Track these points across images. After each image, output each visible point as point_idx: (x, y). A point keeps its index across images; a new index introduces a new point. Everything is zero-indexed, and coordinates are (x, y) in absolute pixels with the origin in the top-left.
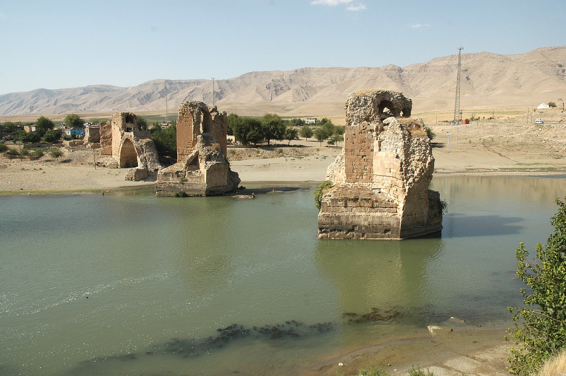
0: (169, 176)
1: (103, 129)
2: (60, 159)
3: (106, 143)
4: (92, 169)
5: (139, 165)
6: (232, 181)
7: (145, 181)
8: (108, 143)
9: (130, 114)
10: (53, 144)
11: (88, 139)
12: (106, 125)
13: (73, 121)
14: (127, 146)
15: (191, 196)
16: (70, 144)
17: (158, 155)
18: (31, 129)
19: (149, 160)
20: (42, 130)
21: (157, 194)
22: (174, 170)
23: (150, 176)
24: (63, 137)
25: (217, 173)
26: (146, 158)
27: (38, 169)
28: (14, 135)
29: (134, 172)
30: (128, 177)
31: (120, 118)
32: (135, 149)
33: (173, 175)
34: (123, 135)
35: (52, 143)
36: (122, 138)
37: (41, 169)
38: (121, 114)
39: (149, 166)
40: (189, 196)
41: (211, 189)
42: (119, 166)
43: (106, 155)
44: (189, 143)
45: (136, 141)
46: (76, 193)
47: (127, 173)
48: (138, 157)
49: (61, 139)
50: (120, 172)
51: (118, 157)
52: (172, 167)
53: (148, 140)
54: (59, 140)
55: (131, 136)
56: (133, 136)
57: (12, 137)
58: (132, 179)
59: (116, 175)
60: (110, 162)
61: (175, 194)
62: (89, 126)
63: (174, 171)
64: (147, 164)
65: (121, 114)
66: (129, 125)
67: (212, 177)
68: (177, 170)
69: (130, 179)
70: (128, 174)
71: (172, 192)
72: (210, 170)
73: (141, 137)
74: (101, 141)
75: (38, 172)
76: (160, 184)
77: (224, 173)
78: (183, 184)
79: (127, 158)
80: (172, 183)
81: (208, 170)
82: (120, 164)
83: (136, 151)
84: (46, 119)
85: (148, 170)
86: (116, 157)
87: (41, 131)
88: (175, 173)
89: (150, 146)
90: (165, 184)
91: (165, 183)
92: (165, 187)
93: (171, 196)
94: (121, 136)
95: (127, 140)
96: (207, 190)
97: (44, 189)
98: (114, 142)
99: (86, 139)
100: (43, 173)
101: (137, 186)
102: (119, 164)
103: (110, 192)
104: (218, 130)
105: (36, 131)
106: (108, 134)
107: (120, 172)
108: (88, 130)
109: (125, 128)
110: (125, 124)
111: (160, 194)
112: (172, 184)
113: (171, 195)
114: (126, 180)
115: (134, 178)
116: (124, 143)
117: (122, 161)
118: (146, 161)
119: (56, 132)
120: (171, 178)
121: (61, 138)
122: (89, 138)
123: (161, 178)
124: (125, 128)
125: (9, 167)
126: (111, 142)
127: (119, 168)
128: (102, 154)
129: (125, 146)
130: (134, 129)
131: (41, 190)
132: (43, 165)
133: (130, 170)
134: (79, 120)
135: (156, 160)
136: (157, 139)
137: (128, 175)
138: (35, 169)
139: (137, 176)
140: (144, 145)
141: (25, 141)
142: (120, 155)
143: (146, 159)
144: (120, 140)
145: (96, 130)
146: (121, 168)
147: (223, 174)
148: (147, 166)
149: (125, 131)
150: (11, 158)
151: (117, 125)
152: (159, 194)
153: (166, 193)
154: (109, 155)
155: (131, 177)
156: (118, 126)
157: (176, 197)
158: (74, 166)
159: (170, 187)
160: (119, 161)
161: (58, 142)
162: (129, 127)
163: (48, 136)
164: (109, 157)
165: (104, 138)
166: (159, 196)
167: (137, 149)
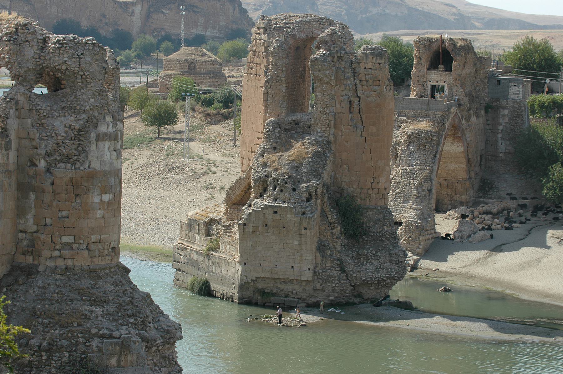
6: (343, 270)
15: (218, 297)
25: (274, 237)
40: (215, 297)
41: (260, 285)
44: (258, 138)
67: (260, 248)
68: (211, 215)
72: (251, 225)
77: (300, 241)
78: (208, 256)
81: (245, 225)
96: (243, 287)
104: (338, 106)
130: (450, 88)
140: (405, 141)
147: (296, 243)
162: (435, 83)
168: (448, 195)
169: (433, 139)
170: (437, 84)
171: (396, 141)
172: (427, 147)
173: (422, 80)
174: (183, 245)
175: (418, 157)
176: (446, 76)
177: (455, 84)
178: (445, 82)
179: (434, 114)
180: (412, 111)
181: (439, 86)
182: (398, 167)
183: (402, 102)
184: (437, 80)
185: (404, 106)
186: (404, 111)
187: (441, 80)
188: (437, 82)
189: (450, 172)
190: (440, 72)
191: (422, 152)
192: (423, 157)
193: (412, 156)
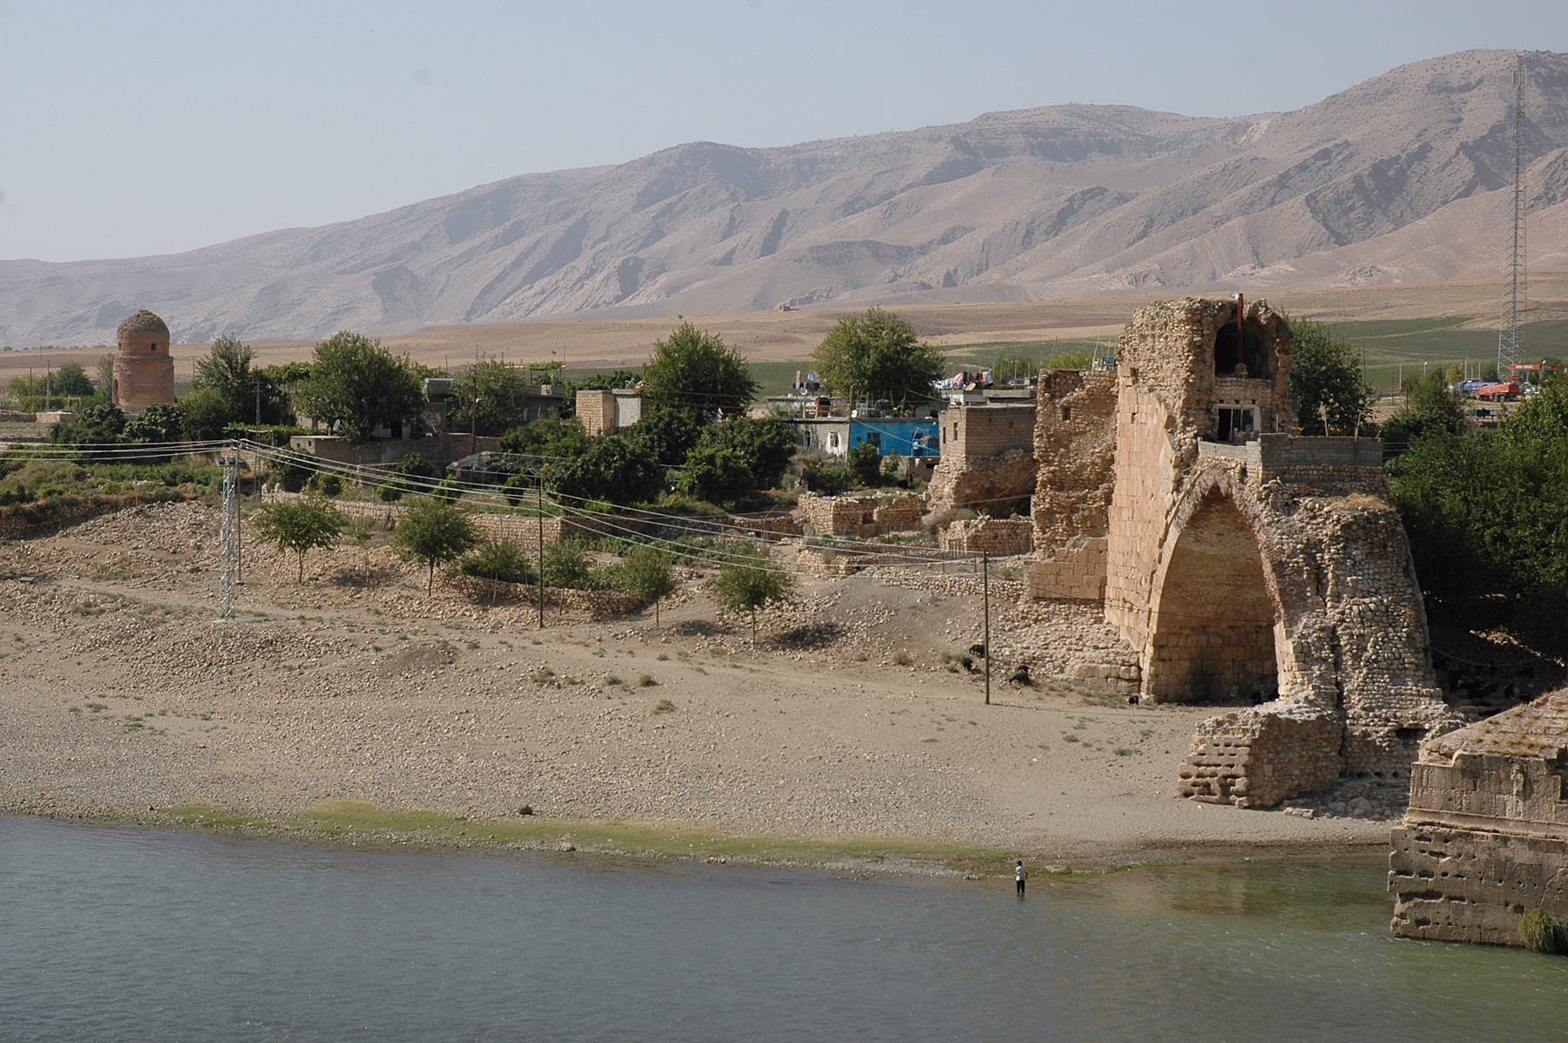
0: (1502, 783)
1: (1060, 415)
2: (768, 618)
3: (1069, 518)
4: (962, 695)
5: (1282, 690)
7: (1315, 815)
8: (1085, 519)
9: (1247, 309)
10: (738, 519)
11: (957, 490)
12: (1079, 393)
13: (869, 363)
14: (1210, 545)
16: (841, 516)
17: (1424, 618)
18: (616, 409)
19: (1356, 658)
20: (680, 420)
21: (1403, 916)
22: (1544, 741)
23: (1361, 775)
24: (801, 467)
26: (1338, 639)
27: (633, 679)
28: (516, 446)
29: (1246, 739)
30: (1199, 776)
31: (1179, 338)
32: (1267, 568)
33: (1528, 784)
34: (1185, 462)
35: (731, 512)
36: (1177, 489)
37: (649, 683)
38: (1182, 315)
39: (1355, 698)
42: (1144, 685)
43: (1060, 601)
45: (1274, 507)
46: (849, 864)
47: (1194, 744)
48: (1279, 630)
49: (783, 482)
50: (1146, 734)
51: (1143, 625)
52: (1526, 720)
53: (1363, 502)
54: (773, 492)
55: (1244, 472)
56: (1256, 469)
57: (505, 459)
58: (1225, 790)
59: (1122, 753)
60: (1088, 653)
61: (1537, 930)
62: (966, 393)
63: (1543, 747)
64: (1339, 685)
65: (1190, 311)
66: (1235, 393)
69: (1215, 786)
70: (1201, 748)
71: (1519, 909)
73: (1311, 484)
74: (1038, 503)
75: (629, 699)
76: (1430, 845)
79: (1203, 629)
80: (1522, 840)
82: (1155, 676)
83: (1272, 586)
84: (707, 348)
85: (1345, 729)
86: (1129, 619)
87: (669, 425)
88: (1549, 762)
89: (1377, 551)
90: (1469, 848)
91: (1467, 836)
92: (1467, 868)
93: (1503, 945)
94: (1172, 473)
95: (1214, 503)
97: (656, 823)
98: (1126, 514)
99: (943, 487)
100: (661, 709)
101: (1259, 846)
102: (1145, 675)
103: (1069, 872)
105: (645, 427)
106: (1087, 454)
107: (1146, 734)
108: (962, 425)
109: (1208, 411)
110: (1205, 384)
111: (1425, 922)
112: (1519, 846)
113: (1507, 938)
114: (1187, 795)
115: (1240, 784)
116: (1194, 521)
117: (1165, 654)
118: (1337, 665)
119: (760, 434)
120: (1512, 805)
121: (786, 477)
122: (964, 479)
123: (1435, 796)
124: (1208, 411)
125: (467, 660)
126: (1103, 513)
127: (1147, 703)
128: (1037, 599)
129: (1196, 548)
130: (1268, 419)
131: (635, 822)
132: (664, 658)
133: (1219, 724)
134: (909, 352)
135: (1409, 658)
136: (1425, 497)
137: (1205, 759)
138: (614, 682)
139: (1268, 769)
140: (1334, 539)
141: (574, 489)
142: (1156, 609)
143: (1335, 648)
144: (1168, 498)
145: (1011, 425)
146: (1160, 702)
148: (1339, 701)
149: (1207, 438)
150: (485, 600)
151: (1151, 390)
152: (1419, 922)
153: (1468, 913)
154: (1086, 602)
155: (1221, 771)
156: (1161, 400)
157: (1542, 951)
158: (851, 675)
159: (1505, 872)
160: (1150, 650)
161: (765, 504)
162: (1233, 406)
163: (711, 460)
164: (1082, 621)
165: (1057, 483)
166: (1418, 932)
167: (1278, 568)
168: (1233, 661)
169: (1398, 529)
170: (1237, 406)
171: (1308, 540)
172: (1389, 549)
173: (1207, 398)
174: (1443, 826)
175: (1374, 574)
176: (1255, 387)
177: (1281, 407)
178: (1254, 402)
179: (1371, 471)
180: (1312, 467)
181: (1237, 412)
182: (1336, 599)
183: (1288, 448)
184: (1237, 397)
185: (1293, 456)
186: (1292, 468)
187: (1245, 398)
188: (1237, 402)
189: (1245, 609)
190: (1243, 380)
191: (1379, 562)
192: (1386, 573)
193: (1361, 573)
